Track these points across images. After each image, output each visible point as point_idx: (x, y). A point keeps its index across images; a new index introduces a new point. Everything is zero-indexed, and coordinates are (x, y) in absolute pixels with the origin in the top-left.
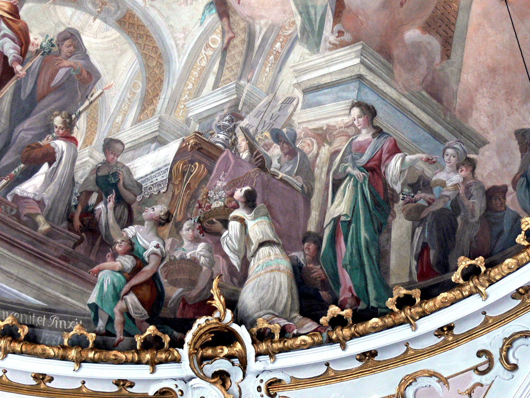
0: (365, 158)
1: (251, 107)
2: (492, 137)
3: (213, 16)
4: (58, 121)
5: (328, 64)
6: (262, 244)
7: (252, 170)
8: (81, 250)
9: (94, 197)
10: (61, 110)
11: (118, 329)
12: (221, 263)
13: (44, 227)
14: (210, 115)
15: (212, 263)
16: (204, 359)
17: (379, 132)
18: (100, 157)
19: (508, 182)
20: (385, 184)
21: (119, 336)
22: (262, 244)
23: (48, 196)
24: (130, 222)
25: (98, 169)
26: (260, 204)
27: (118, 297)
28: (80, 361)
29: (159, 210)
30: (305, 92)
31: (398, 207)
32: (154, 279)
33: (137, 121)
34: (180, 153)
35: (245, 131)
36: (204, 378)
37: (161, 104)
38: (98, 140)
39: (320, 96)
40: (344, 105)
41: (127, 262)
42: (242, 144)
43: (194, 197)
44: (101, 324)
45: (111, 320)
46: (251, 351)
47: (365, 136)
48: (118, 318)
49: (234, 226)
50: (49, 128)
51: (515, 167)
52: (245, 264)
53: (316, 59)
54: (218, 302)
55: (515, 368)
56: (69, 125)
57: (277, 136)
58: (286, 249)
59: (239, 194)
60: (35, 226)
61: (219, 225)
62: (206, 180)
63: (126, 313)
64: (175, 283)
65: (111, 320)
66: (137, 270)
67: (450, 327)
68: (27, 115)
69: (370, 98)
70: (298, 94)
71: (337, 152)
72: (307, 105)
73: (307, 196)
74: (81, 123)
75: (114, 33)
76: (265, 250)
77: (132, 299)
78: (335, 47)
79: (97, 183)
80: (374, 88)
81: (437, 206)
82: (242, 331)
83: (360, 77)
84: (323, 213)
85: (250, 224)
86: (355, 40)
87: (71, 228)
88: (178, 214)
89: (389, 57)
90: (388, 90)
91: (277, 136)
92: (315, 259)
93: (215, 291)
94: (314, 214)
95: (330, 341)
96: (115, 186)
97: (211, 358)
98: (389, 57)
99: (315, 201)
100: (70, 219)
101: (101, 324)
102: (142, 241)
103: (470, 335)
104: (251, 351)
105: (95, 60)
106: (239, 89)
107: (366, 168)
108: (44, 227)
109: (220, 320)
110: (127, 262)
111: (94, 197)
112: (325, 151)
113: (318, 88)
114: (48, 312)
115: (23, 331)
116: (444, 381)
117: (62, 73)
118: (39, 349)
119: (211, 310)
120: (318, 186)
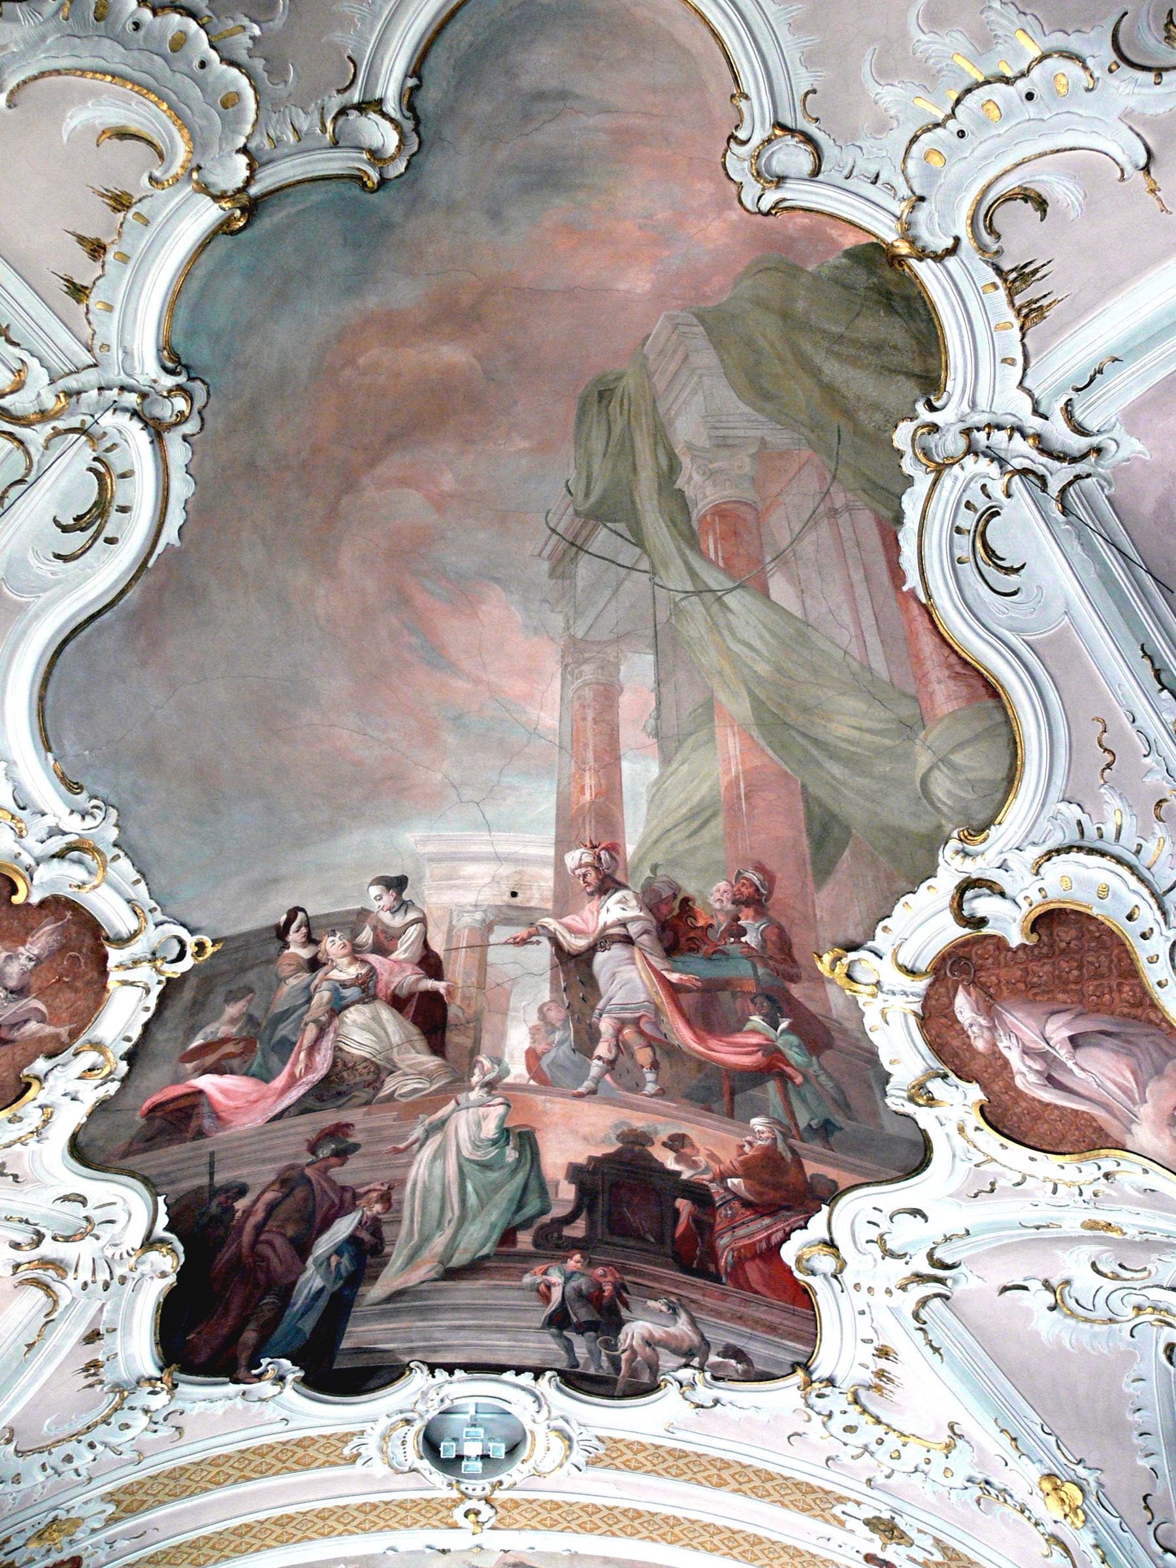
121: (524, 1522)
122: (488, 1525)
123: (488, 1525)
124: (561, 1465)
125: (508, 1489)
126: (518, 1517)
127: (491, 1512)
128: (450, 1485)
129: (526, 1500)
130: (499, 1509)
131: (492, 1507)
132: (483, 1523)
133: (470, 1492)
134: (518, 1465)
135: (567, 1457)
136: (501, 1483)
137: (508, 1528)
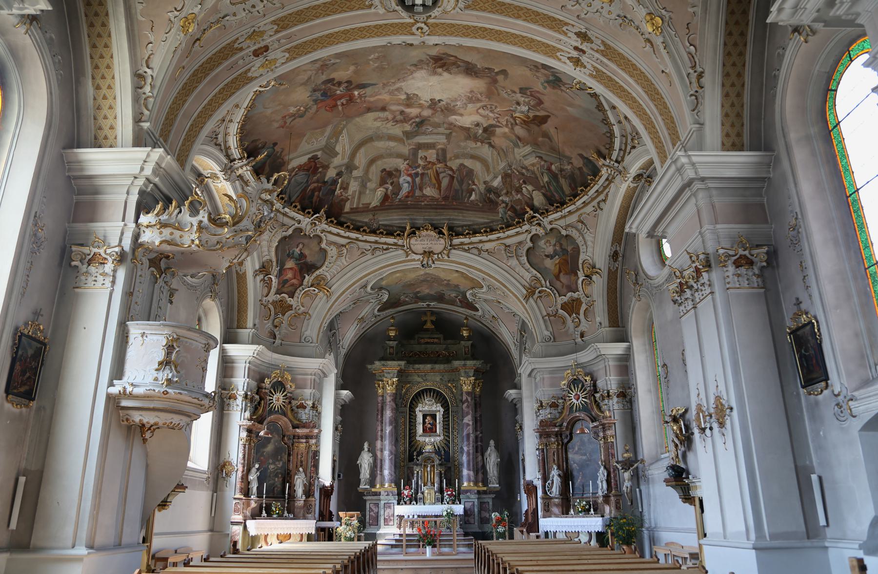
0: (546, 168)
1: (513, 164)
2: (572, 156)
3: (491, 149)
4: (470, 182)
5: (525, 150)
6: (533, 191)
7: (521, 176)
8: (492, 206)
9: (488, 195)
10: (469, 180)
11: (510, 220)
12: (526, 198)
13: (481, 205)
14: (504, 168)
15: (523, 198)
16: (531, 223)
17: (545, 161)
18: (484, 186)
19: (582, 166)
20: (554, 173)
21: (511, 222)
22: (533, 191)
23: (477, 198)
24: (500, 197)
25: (485, 189)
26: (527, 183)
27: (506, 213)
28: (504, 232)
29: (505, 191)
30: (523, 157)
31: (559, 176)
32: (512, 206)
33: (488, 176)
34: (502, 177)
35: (514, 169)
36: (534, 226)
37: (491, 169)
38: (482, 182)
39: (527, 157)
40: (533, 158)
41: (504, 205)
42: (516, 171)
43: (511, 185)
44: (505, 220)
45: (507, 219)
46: (541, 218)
47: (543, 163)
48: (508, 218)
49: (524, 189)
50: (469, 184)
51: (582, 162)
52: (531, 196)
53: (521, 150)
54: (528, 209)
55: (602, 209)
56: (473, 182)
57: (523, 168)
58: (539, 190)
59: (521, 182)
60: (479, 205)
61: (520, 190)
62: (512, 181)
63: (509, 216)
64: (517, 205)
65: (507, 219)
66: (507, 205)
67: (584, 202)
68: (463, 184)
69: (539, 155)
70: (521, 158)
71: (538, 168)
72: (525, 160)
73: (537, 178)
74: (476, 180)
75: (471, 160)
76: (534, 192)
77: (509, 212)
78: (524, 146)
79: (487, 191)
80: (538, 152)
81: (568, 174)
82: (536, 215)
83: (534, 151)
84: (543, 181)
85: (528, 187)
86: (528, 144)
87: (487, 203)
88: (509, 190)
89: (538, 145)
90: (542, 152)
91: (523, 168)
92: (547, 191)
93: (526, 208)
94: (541, 182)
95: (557, 212)
96: (491, 190)
97: (534, 221)
98: (538, 145)
99: (539, 179)
100: (486, 201)
101: (505, 220)
102: (504, 199)
103: (589, 203)
104: (541, 218)
105: (470, 167)
106: (507, 161)
107: (547, 170)
108: (481, 205)
109: (530, 214)
110: (504, 205)
111: (488, 195)
112: (535, 168)
113: (525, 156)
114: (492, 222)
115: (488, 230)
116: (588, 214)
117: (465, 173)
118: (494, 233)
119: (527, 212)
120: (538, 176)
121: (441, 32)
122: (427, 33)
123: (427, 33)
124: (454, 9)
125: (433, 19)
126: (438, 31)
127: (427, 28)
128: (410, 17)
129: (441, 23)
130: (430, 27)
131: (428, 26)
132: (425, 33)
133: (418, 20)
134: (437, 9)
135: (456, 5)
136: (430, 16)
137: (434, 35)
